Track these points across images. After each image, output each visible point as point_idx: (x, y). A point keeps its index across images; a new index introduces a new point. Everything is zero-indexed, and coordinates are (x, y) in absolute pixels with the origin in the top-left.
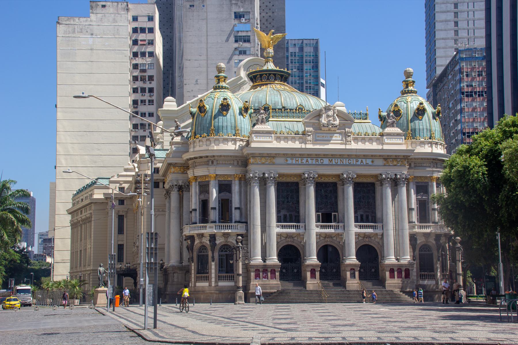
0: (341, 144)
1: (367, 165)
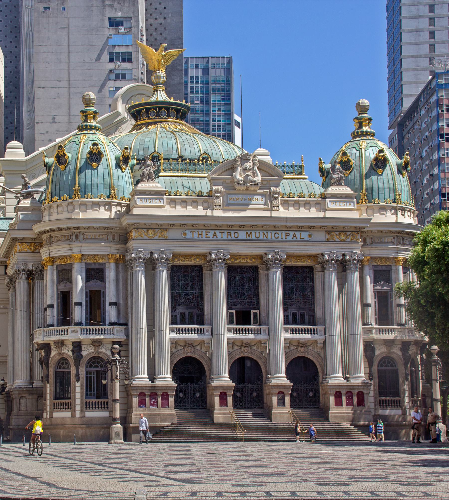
0: (264, 210)
1: (302, 240)
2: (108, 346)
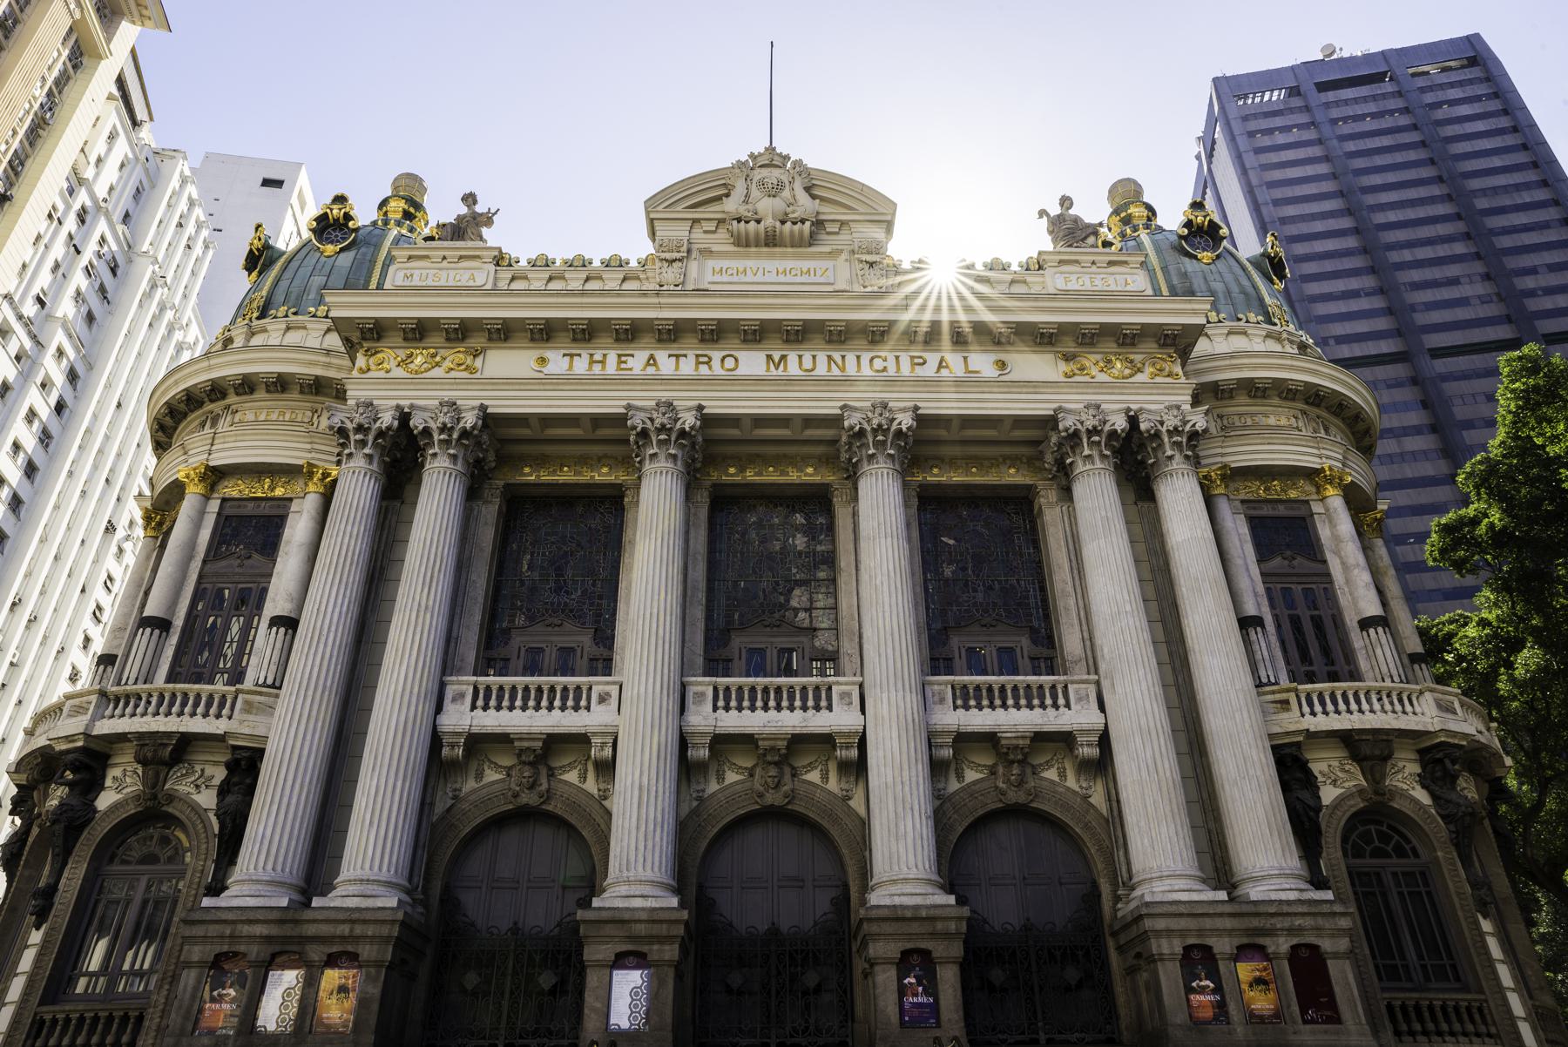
2: (209, 770)
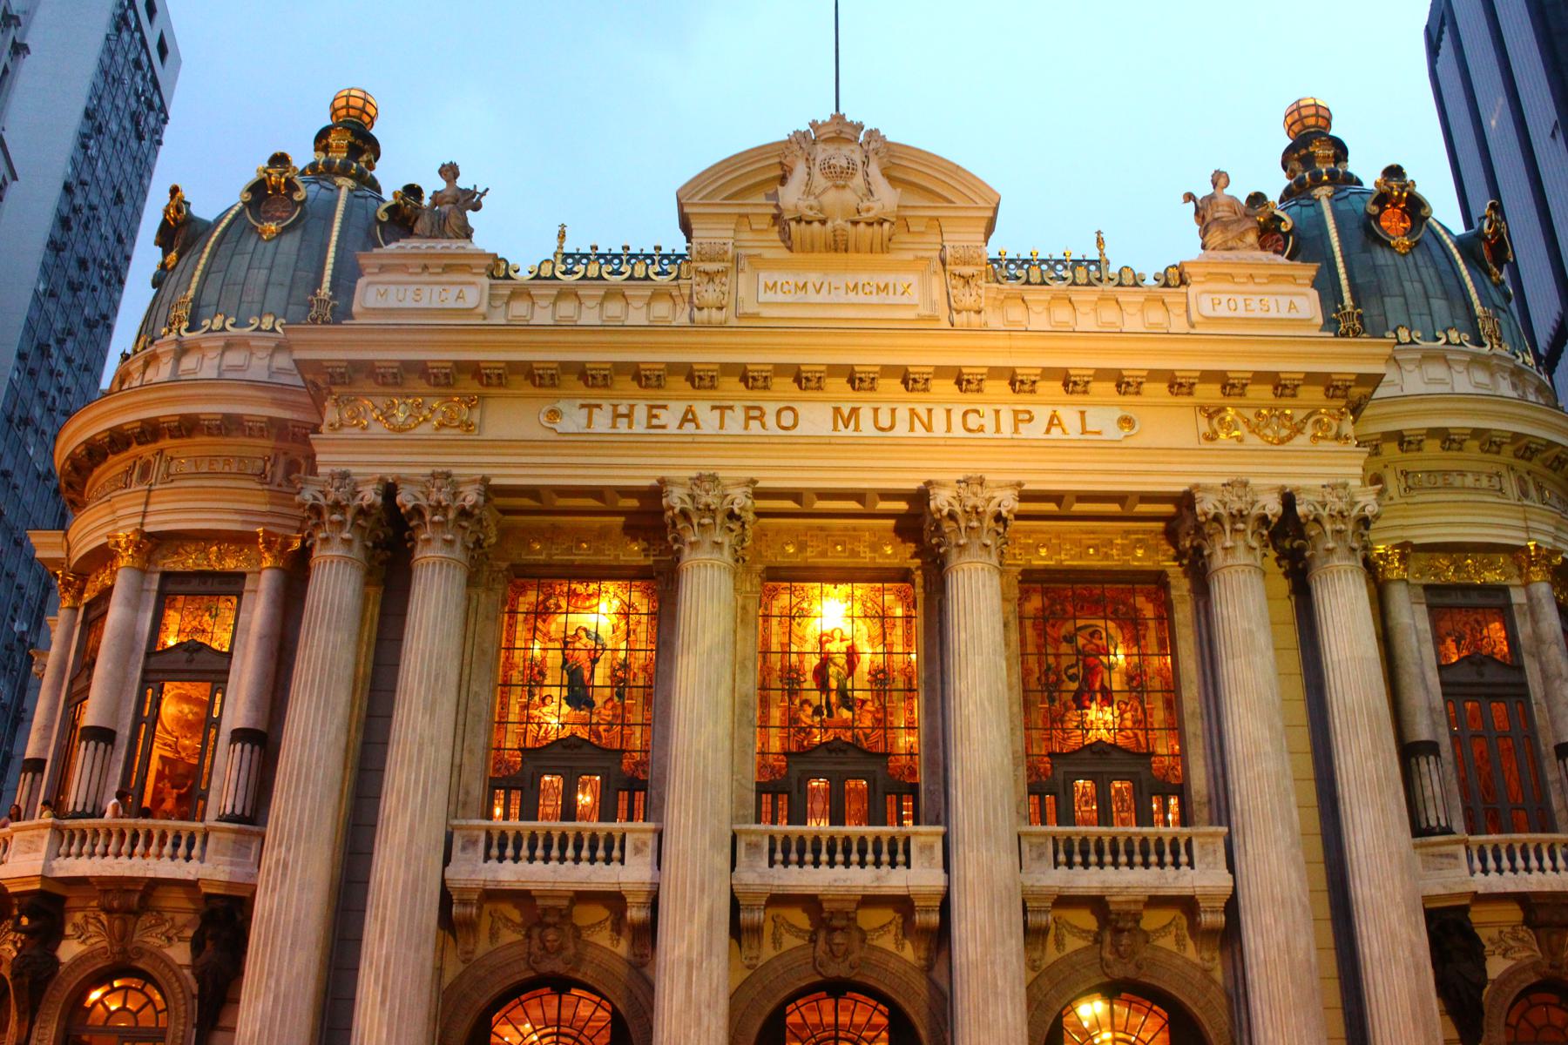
2: (181, 919)
